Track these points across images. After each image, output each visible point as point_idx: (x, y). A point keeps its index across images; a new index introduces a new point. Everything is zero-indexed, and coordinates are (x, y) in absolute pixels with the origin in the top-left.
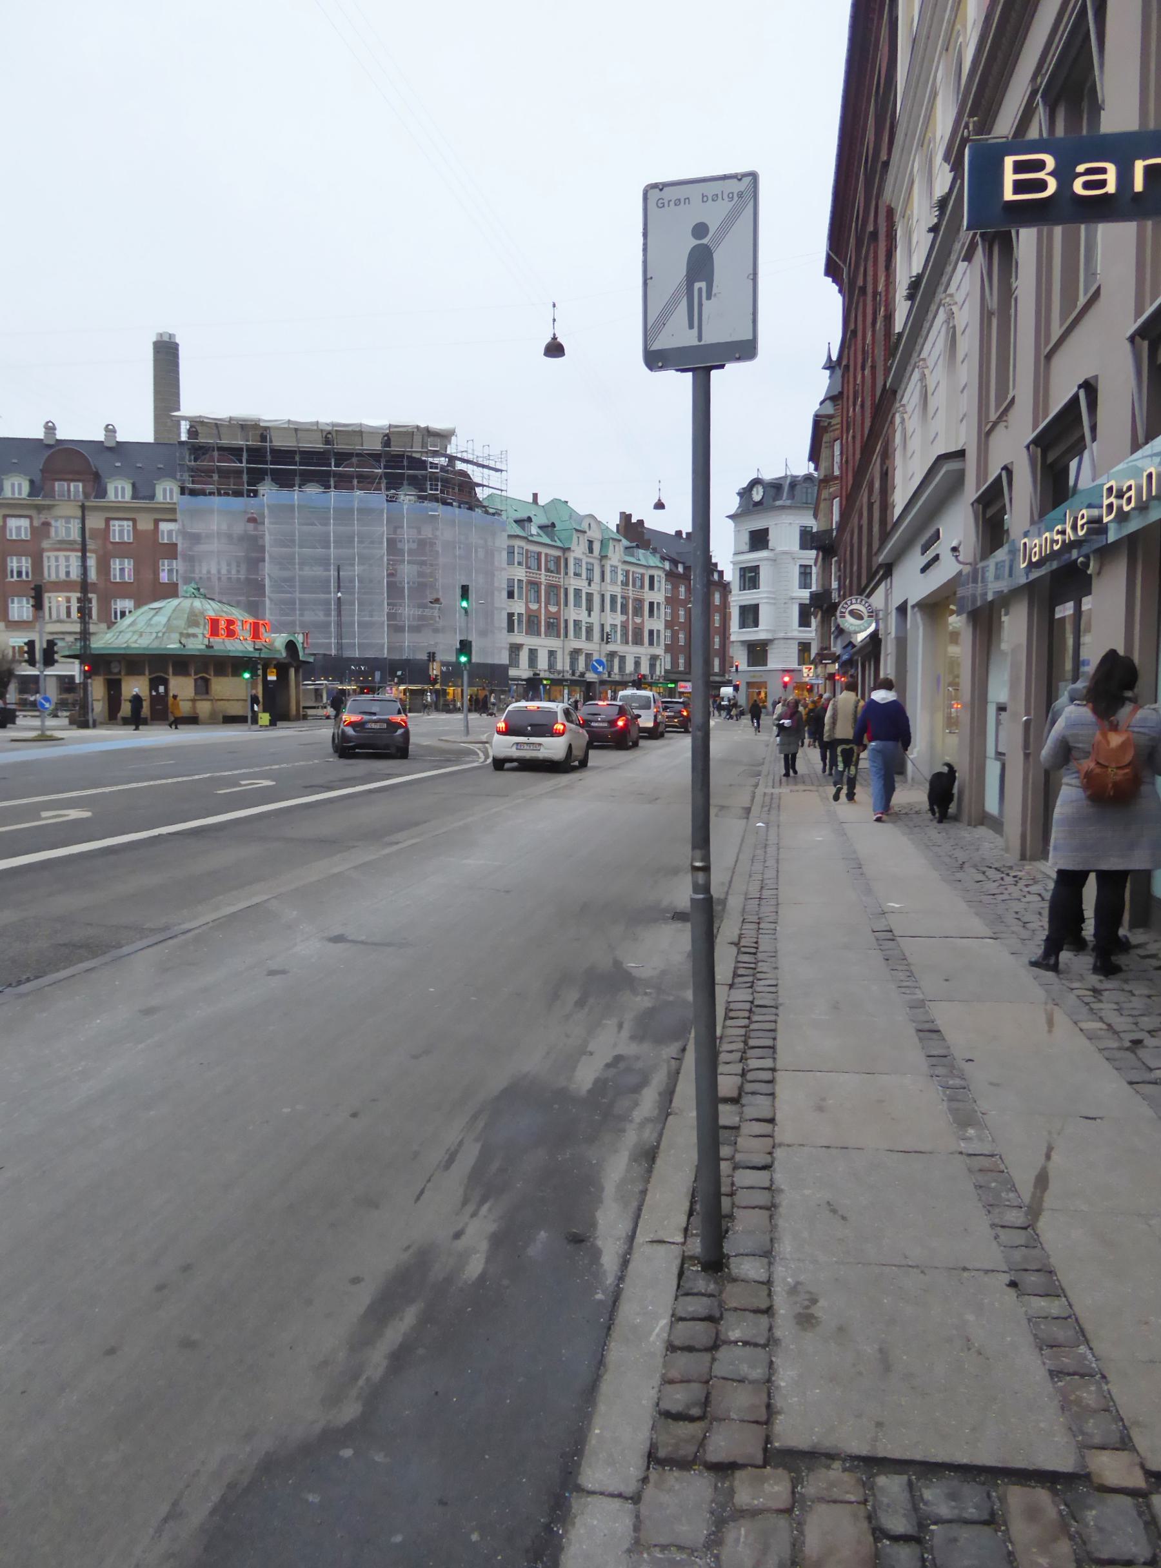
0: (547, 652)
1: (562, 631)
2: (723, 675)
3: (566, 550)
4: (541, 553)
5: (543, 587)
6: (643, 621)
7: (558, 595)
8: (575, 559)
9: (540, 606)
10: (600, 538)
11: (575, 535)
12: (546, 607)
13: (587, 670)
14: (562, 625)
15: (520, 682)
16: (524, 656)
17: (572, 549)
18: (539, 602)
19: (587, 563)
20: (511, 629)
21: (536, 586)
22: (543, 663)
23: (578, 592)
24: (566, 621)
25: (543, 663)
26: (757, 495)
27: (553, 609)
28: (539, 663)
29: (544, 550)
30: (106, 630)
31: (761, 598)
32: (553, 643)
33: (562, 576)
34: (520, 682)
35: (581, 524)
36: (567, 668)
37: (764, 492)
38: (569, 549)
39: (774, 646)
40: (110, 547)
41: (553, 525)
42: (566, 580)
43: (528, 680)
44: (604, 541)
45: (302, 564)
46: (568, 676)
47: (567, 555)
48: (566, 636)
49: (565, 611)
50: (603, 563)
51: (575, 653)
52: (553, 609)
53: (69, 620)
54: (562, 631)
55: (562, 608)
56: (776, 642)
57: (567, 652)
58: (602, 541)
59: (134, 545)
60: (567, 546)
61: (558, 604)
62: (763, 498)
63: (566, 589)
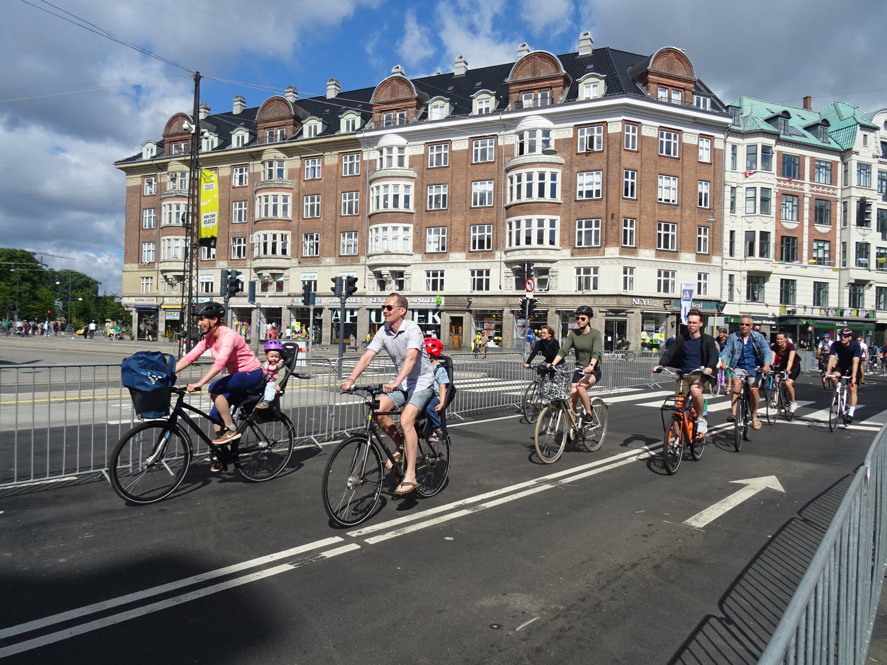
0: (812, 284)
1: (838, 257)
3: (845, 154)
5: (806, 200)
8: (860, 164)
9: (802, 224)
11: (860, 133)
12: (811, 225)
13: (878, 308)
14: (838, 249)
15: (764, 322)
16: (772, 290)
17: (855, 149)
18: (800, 218)
19: (880, 172)
21: (796, 199)
23: (863, 206)
25: (804, 297)
28: (798, 298)
29: (809, 153)
30: (297, 265)
33: (839, 186)
34: (764, 322)
35: (871, 121)
38: (849, 150)
40: (303, 184)
41: (826, 123)
43: (781, 319)
45: (389, 157)
53: (274, 256)
54: (838, 257)
59: (322, 181)
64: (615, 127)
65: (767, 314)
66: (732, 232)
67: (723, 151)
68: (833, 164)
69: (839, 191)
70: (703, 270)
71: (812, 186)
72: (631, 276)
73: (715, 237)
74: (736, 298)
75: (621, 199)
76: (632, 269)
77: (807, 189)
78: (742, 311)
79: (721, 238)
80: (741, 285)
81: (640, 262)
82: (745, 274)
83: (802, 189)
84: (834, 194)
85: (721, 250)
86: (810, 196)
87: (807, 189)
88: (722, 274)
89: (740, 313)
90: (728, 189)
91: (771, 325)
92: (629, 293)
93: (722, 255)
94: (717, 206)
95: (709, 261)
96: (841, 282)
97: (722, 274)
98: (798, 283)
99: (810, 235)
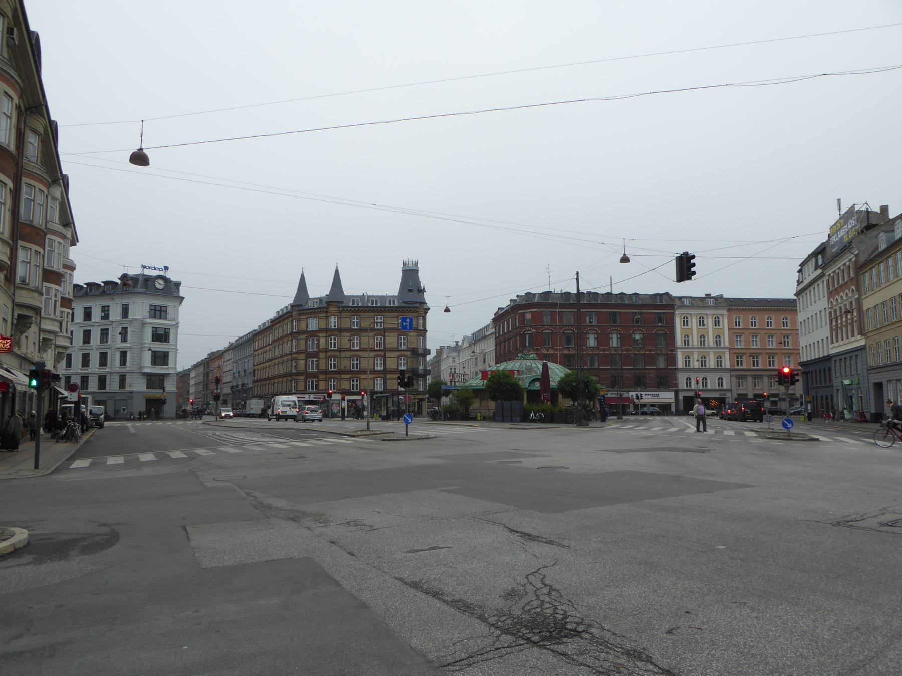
26: (160, 285)
31: (172, 348)
39: (168, 378)
62: (164, 287)
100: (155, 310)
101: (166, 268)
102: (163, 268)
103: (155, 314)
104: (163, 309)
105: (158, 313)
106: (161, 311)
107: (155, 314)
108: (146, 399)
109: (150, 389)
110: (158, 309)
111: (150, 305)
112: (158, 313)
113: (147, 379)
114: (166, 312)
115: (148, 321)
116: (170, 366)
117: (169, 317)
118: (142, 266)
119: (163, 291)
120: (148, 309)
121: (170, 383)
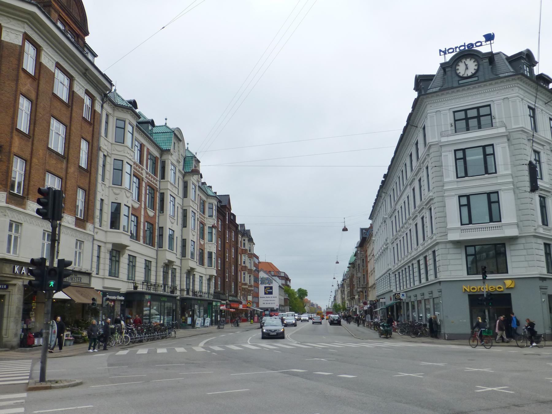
2: (236, 296)
4: (144, 145)
5: (144, 184)
6: (204, 244)
7: (153, 198)
9: (141, 205)
10: (184, 156)
20: (115, 223)
22: (140, 276)
24: (161, 229)
27: (151, 213)
32: (149, 252)
33: (158, 179)
36: (161, 282)
37: (478, 65)
39: (513, 247)
42: (162, 183)
43: (128, 295)
44: (186, 160)
46: (160, 291)
47: (164, 157)
48: (161, 246)
49: (161, 217)
50: (186, 179)
51: (168, 265)
52: (151, 213)
55: (157, 211)
56: (523, 241)
57: (161, 264)
58: (185, 159)
60: (164, 147)
61: (153, 208)
62: (477, 71)
63: (162, 195)
64: (13, 36)
65: (119, 289)
66: (102, 200)
67: (100, 115)
68: (156, 158)
69: (158, 183)
70: (81, 237)
71: (147, 173)
72: (10, 233)
73: (90, 203)
74: (101, 272)
75: (14, 131)
76: (19, 224)
77: (144, 172)
78: (106, 286)
79: (94, 205)
80: (105, 257)
81: (28, 218)
82: (110, 247)
83: (142, 174)
84: (156, 184)
85: (93, 218)
86: (146, 182)
87: (144, 172)
88: (93, 244)
89: (104, 287)
90: (101, 155)
91: (121, 301)
92: (11, 256)
93: (93, 223)
94: (93, 169)
95: (84, 228)
96: (159, 261)
97: (93, 244)
98: (138, 259)
99: (145, 217)
100: (467, 119)
101: (489, 37)
102: (483, 39)
103: (467, 125)
104: (483, 111)
105: (473, 123)
106: (478, 117)
107: (467, 125)
108: (470, 296)
109: (498, 273)
110: (473, 113)
111: (454, 112)
112: (473, 123)
113: (467, 256)
114: (490, 114)
115: (444, 139)
116: (504, 221)
117: (496, 121)
118: (440, 51)
119: (476, 79)
120: (450, 119)
121: (523, 258)
